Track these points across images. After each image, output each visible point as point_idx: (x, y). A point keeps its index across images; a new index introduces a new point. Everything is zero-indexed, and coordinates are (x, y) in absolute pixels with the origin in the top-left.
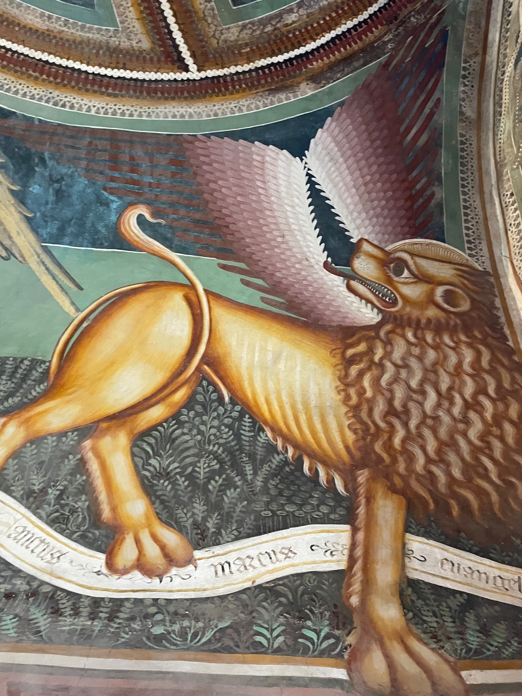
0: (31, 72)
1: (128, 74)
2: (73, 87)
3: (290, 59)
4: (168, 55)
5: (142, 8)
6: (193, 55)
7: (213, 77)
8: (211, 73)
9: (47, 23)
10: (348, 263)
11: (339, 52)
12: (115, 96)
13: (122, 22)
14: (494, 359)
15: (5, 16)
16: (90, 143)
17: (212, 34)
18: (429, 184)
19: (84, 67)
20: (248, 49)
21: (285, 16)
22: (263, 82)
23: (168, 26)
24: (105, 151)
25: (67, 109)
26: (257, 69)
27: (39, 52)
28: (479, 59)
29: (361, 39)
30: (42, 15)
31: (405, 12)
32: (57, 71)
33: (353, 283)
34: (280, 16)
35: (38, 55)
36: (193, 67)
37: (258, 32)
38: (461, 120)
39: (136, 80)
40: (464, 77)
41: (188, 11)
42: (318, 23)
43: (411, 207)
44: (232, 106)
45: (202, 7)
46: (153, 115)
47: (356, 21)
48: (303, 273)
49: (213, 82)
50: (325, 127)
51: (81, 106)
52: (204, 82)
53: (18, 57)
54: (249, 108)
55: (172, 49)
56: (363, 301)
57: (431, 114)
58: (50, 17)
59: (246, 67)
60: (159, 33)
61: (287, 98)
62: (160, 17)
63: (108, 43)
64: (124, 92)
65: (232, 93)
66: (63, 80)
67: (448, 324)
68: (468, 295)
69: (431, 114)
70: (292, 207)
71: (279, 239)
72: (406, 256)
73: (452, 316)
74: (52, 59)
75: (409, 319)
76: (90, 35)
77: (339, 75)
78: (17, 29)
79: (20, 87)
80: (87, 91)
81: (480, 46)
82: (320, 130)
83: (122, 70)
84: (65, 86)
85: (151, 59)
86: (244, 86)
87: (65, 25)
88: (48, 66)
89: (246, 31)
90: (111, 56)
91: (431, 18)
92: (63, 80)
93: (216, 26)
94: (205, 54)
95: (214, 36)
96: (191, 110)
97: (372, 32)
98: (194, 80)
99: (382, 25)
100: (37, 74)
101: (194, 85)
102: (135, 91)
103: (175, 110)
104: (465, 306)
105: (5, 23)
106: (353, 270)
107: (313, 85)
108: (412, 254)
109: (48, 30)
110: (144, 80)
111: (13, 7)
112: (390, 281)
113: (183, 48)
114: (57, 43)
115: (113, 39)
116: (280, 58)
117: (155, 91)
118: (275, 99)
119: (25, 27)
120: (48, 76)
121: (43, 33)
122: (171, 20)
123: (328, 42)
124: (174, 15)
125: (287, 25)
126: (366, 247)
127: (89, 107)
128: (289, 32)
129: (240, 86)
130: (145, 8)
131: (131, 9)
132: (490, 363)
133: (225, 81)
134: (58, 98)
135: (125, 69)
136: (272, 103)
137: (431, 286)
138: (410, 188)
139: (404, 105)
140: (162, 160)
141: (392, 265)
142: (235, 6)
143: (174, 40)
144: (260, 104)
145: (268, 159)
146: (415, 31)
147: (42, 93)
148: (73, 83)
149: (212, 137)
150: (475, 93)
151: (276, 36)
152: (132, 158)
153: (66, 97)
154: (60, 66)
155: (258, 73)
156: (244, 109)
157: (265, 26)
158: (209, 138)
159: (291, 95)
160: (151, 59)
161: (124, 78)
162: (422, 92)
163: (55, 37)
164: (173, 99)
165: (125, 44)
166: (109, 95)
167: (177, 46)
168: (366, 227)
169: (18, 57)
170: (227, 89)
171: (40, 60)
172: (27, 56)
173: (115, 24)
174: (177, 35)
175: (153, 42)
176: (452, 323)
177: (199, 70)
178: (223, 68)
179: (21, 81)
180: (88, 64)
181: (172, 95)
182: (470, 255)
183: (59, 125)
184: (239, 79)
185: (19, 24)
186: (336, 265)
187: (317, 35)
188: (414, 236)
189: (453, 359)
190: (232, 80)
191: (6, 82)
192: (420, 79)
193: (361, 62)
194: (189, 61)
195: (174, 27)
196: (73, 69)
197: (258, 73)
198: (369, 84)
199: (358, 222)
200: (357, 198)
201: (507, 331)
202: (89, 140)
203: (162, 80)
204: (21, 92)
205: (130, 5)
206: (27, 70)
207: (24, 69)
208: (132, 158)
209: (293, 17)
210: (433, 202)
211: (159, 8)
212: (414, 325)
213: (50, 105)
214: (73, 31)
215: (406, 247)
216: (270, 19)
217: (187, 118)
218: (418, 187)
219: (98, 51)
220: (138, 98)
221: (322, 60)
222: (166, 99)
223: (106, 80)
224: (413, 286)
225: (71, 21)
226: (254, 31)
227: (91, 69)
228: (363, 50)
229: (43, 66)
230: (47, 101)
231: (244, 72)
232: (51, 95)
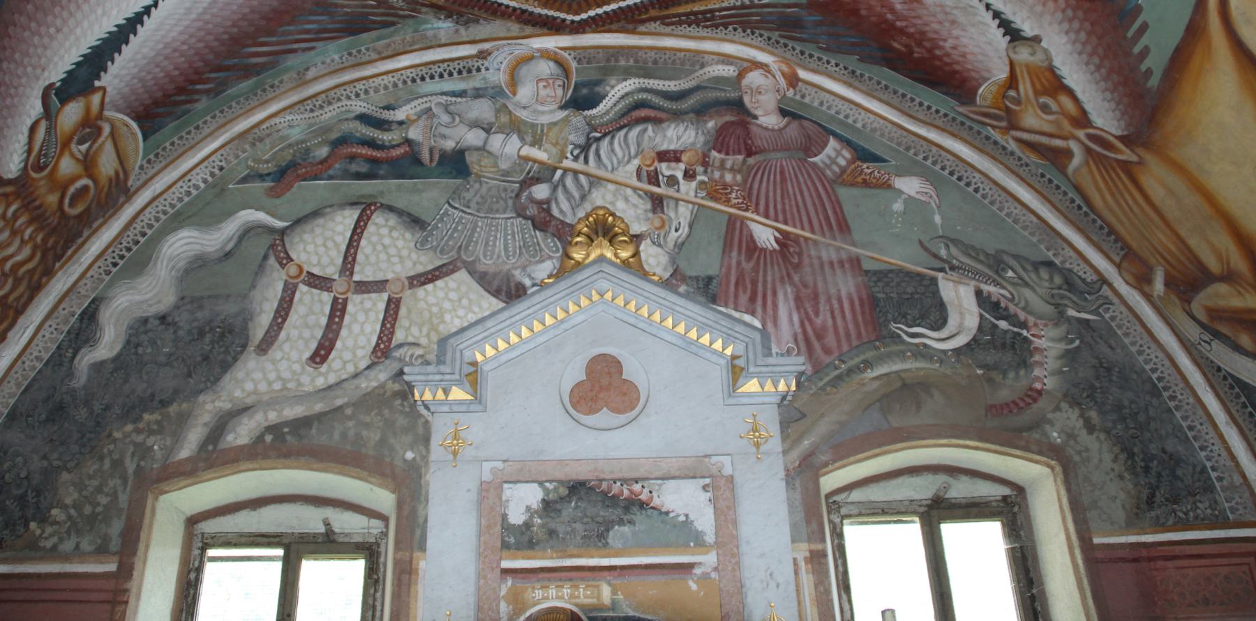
10: (64, 102)
14: (31, 272)
18: (207, 92)
28: (374, 56)
33: (43, 124)
38: (299, 73)
40: (350, 54)
43: (171, 96)
48: (24, 80)
56: (26, 148)
67: (46, 219)
68: (92, 201)
70: (104, 14)
71: (52, 30)
72: (107, 129)
73: (58, 214)
75: (32, 193)
81: (389, 53)
91: (402, 10)
104: (75, 212)
106: (59, 111)
108: (113, 135)
112: (66, 144)
126: (96, 99)
132: (28, 271)
137: (83, 173)
138: (193, 82)
139: (291, 28)
141: (88, 130)
150: (337, 67)
162: (316, 33)
168: (121, 81)
176: (50, 220)
182: (141, 167)
186: (56, 95)
188: (137, 118)
189: (10, 251)
192: (329, 26)
199: (124, 72)
200: (153, 53)
201: (70, 252)
210: (188, 106)
212: (26, 201)
215: (117, 123)
218: (199, 87)
224: (73, 162)
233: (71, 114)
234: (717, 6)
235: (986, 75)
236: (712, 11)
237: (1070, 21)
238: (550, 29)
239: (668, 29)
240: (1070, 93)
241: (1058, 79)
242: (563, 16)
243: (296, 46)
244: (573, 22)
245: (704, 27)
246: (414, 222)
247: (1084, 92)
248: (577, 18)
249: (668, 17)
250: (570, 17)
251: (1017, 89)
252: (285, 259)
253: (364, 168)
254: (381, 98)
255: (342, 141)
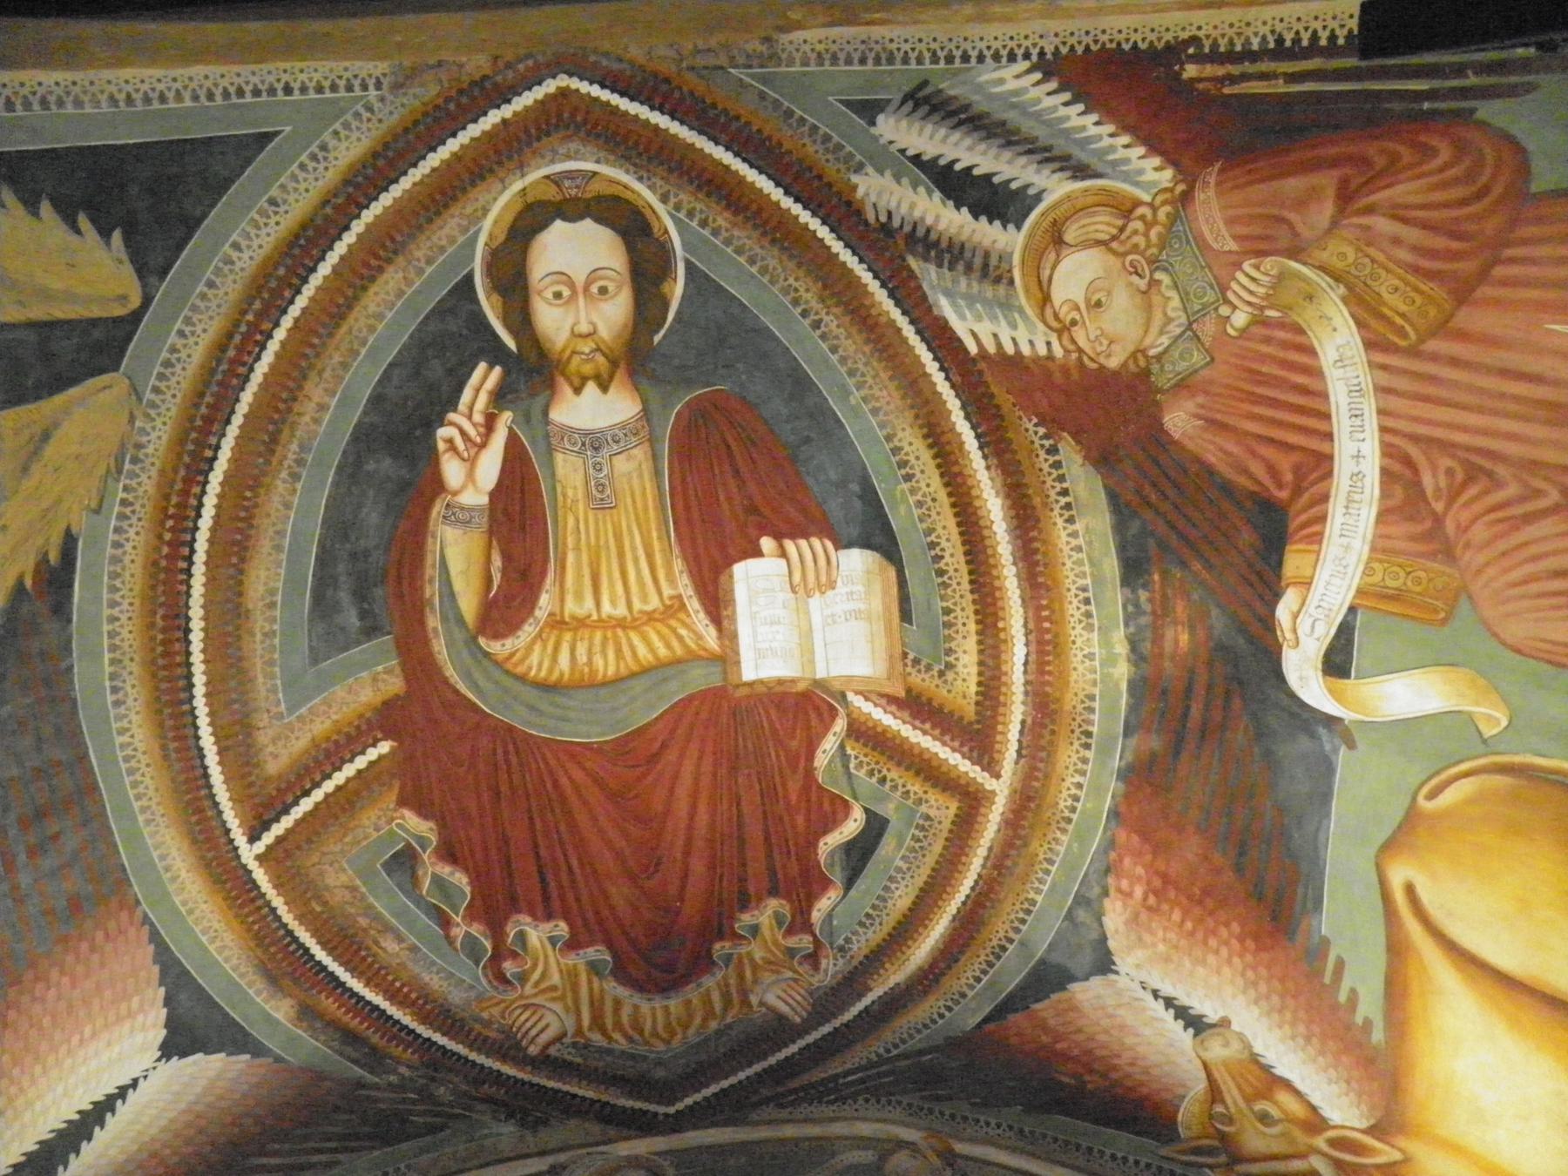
0: (161, 612)
1: (212, 759)
2: (157, 689)
3: (324, 968)
4: (268, 805)
5: (335, 737)
6: (280, 840)
7: (254, 882)
8: (260, 876)
9: (260, 604)
11: (361, 1023)
12: (166, 757)
13: (301, 719)
15: (253, 532)
16: (59, 763)
17: (325, 849)
19: (199, 690)
20: (318, 909)
21: (390, 936)
22: (272, 950)
23: (317, 785)
24: (53, 791)
25: (110, 698)
26: (290, 933)
27: (201, 612)
29: (389, 1041)
30: (273, 592)
31: (451, 1076)
32: (178, 653)
34: (387, 928)
35: (196, 613)
36: (260, 847)
37: (353, 911)
39: (206, 776)
41: (352, 804)
42: (394, 981)
44: (216, 925)
45: (367, 823)
46: (152, 828)
47: (413, 1025)
49: (246, 883)
50: (234, 1058)
51: (126, 716)
52: (241, 872)
53: (181, 582)
54: (221, 950)
55: (279, 807)
57: (311, 1166)
58: (272, 605)
59: (288, 918)
60: (300, 777)
61: (259, 993)
62: (328, 769)
63: (256, 710)
64: (177, 766)
65: (236, 916)
66: (164, 668)
69: (311, 1166)
74: (197, 638)
76: (260, 680)
77: (322, 1038)
78: (234, 560)
79: (125, 606)
80: (159, 712)
82: (222, 1055)
83: (215, 748)
84: (154, 676)
85: (251, 785)
86: (256, 927)
87: (266, 635)
88: (180, 634)
89: (346, 892)
90: (234, 723)
92: (164, 668)
93: (342, 851)
94: (288, 854)
95: (324, 854)
96: (183, 874)
97: (405, 1050)
98: (238, 857)
99: (421, 1057)
100: (160, 623)
101: (232, 860)
102: (186, 782)
103: (174, 852)
105: (239, 537)
107: (292, 1013)
109: (248, 611)
110: (210, 787)
111: (272, 539)
113: (287, 822)
114: (229, 634)
115: (266, 716)
116: (320, 954)
117: (200, 811)
118: (252, 977)
119: (241, 572)
120: (164, 643)
121: (239, 605)
122: (329, 786)
123: (369, 1003)
124: (339, 788)
125: (376, 943)
127: (128, 730)
128: (368, 949)
129: (254, 923)
130: (336, 742)
131: (328, 724)
133: (253, 900)
134: (125, 674)
135: (219, 753)
136: (242, 976)
140: (73, 883)
142: (383, 865)
143: (296, 803)
144: (235, 961)
145: (140, 1018)
146: (426, 1096)
147: (126, 644)
148: (164, 686)
149: (147, 927)
151: (356, 935)
152: (55, 837)
153: (133, 686)
154: (188, 654)
155: (284, 937)
156: (218, 944)
157: (366, 915)
158: (143, 924)
159: (265, 994)
160: (251, 785)
161: (202, 757)
163: (238, 628)
164: (194, 842)
165: (263, 738)
166: (164, 747)
167: (286, 811)
169: (181, 582)
170: (241, 906)
171: (188, 619)
172: (189, 595)
173: (291, 710)
174: (306, 805)
175: (280, 776)
177: (259, 858)
178: (275, 887)
179: (137, 602)
180: (207, 695)
181: (201, 837)
183: (74, 701)
184: (265, 917)
185: (243, 560)
187: (377, 986)
190: (260, 908)
191: (128, 578)
193: (355, 1055)
194: (268, 838)
195: (318, 795)
196: (189, 676)
197: (284, 937)
198: (325, 1079)
202: (64, 758)
203: (220, 813)
204: (115, 612)
205: (334, 717)
206: (161, 605)
207: (162, 599)
208: (55, 837)
209: (390, 945)
211: (343, 762)
213: (108, 669)
214: (259, 652)
216: (377, 917)
217: (166, 876)
219: (235, 701)
220: (175, 791)
221: (339, 1007)
222: (191, 833)
223: (189, 731)
225: (277, 641)
226: (352, 904)
227: (200, 703)
228: (374, 1049)
229: (179, 628)
230: (113, 662)
231: (278, 918)
232: (127, 662)
234: (839, 1070)
235: (1180, 1091)
236: (836, 1076)
237: (1255, 984)
238: (640, 1128)
239: (784, 1114)
240: (1287, 1085)
241: (1266, 1069)
242: (653, 1108)
243: (315, 1158)
244: (666, 1115)
245: (828, 1102)
247: (1303, 1080)
248: (671, 1110)
249: (783, 1095)
250: (662, 1110)
251: (1223, 1102)
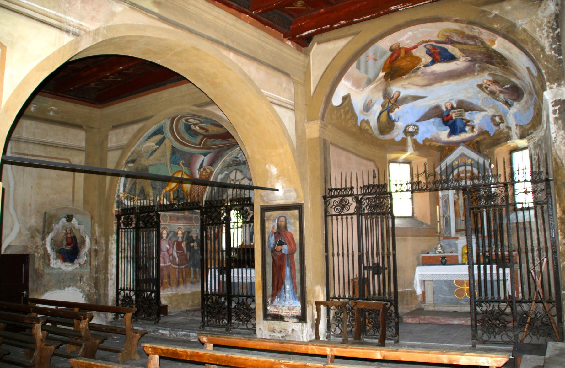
233: (202, 170)
246: (241, 171)
252: (229, 178)
253: (235, 164)
254: (237, 154)
255: (233, 161)
